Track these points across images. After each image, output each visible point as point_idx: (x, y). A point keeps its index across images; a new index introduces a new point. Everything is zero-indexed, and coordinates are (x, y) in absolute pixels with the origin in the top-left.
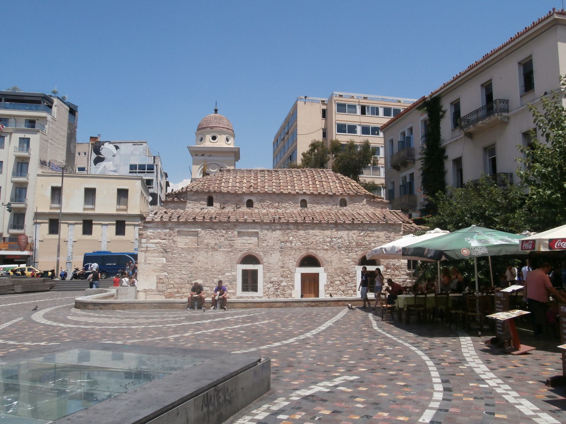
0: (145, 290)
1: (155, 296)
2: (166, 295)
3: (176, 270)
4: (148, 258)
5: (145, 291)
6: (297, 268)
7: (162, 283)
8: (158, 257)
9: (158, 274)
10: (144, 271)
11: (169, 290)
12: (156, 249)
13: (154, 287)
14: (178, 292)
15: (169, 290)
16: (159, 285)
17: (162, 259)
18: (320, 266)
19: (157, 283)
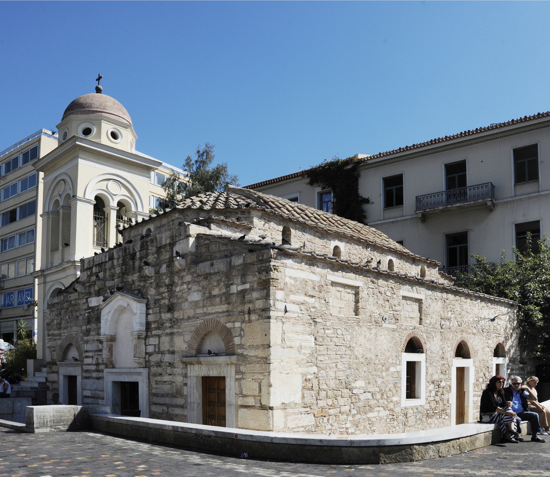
0: (283, 404)
1: (300, 416)
2: (315, 414)
3: (330, 362)
4: (288, 335)
5: (284, 406)
6: (454, 360)
7: (309, 390)
8: (304, 334)
9: (304, 370)
10: (282, 364)
11: (321, 403)
12: (300, 315)
13: (298, 399)
14: (332, 406)
15: (321, 403)
16: (307, 393)
17: (309, 337)
18: (470, 358)
19: (304, 388)
